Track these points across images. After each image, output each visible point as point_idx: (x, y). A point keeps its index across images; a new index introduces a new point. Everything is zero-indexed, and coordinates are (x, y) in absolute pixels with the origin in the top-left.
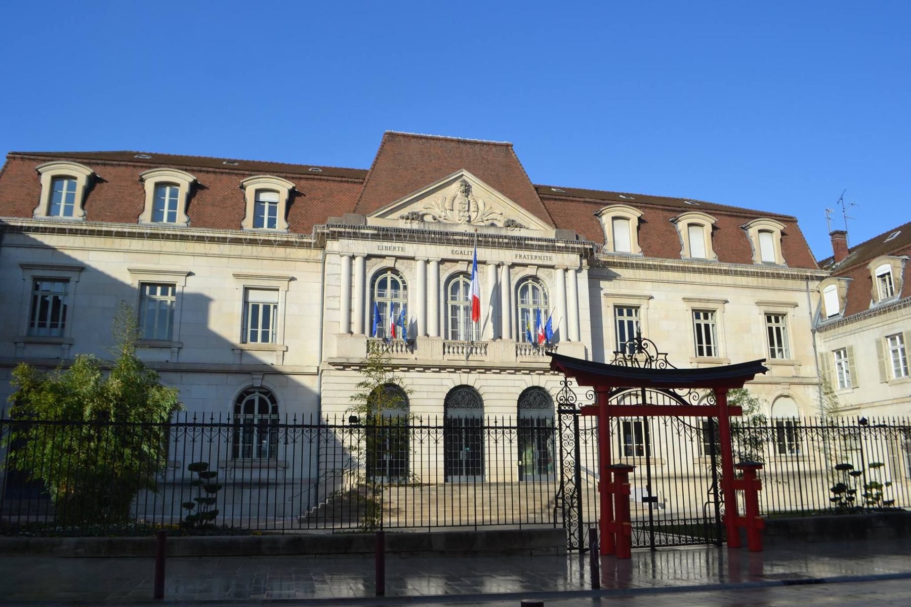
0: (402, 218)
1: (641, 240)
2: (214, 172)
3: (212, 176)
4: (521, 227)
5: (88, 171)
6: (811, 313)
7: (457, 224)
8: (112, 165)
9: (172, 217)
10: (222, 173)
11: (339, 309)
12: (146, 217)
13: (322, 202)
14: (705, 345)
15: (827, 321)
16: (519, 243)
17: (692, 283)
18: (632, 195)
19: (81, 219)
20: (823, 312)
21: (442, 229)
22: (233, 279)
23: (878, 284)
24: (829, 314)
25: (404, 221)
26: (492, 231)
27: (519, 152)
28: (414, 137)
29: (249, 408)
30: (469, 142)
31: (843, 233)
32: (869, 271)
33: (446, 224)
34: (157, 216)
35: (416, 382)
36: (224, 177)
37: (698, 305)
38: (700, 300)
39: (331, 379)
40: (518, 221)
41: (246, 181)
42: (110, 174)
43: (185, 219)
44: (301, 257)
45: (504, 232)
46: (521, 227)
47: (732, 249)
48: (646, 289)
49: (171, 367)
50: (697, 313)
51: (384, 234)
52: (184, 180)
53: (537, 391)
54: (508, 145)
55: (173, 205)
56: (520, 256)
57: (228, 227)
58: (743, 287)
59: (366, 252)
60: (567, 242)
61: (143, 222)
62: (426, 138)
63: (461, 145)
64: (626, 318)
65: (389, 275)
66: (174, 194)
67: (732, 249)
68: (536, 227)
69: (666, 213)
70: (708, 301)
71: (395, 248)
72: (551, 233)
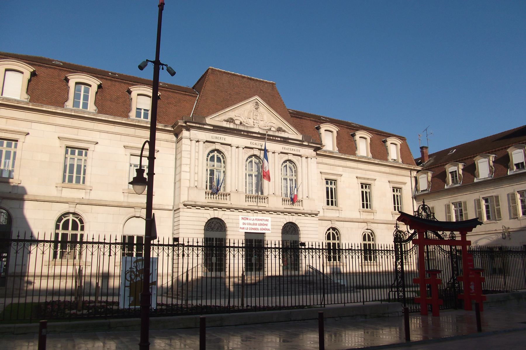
1: (339, 144)
2: (111, 80)
3: (109, 82)
4: (284, 131)
5: (31, 69)
7: (253, 127)
8: (46, 67)
9: (85, 106)
10: (116, 81)
11: (190, 172)
12: (69, 104)
13: (175, 106)
14: (365, 203)
15: (420, 193)
16: (285, 141)
18: (328, 118)
19: (94, 112)
21: (246, 129)
22: (124, 149)
23: (450, 176)
24: (421, 189)
25: (226, 122)
26: (270, 133)
27: (279, 88)
28: (224, 72)
29: (66, 226)
30: (253, 80)
31: (427, 148)
32: (445, 169)
33: (248, 127)
34: (76, 104)
35: (231, 217)
36: (117, 83)
38: (364, 179)
39: (185, 214)
40: (284, 128)
41: (132, 89)
42: (44, 73)
43: (95, 108)
44: (163, 138)
45: (277, 134)
46: (284, 131)
47: (379, 153)
48: (339, 171)
49: (86, 202)
50: (362, 185)
51: (217, 129)
52: (94, 83)
53: (216, 220)
54: (273, 84)
55: (86, 98)
57: (121, 116)
58: (384, 173)
59: (205, 139)
60: (309, 142)
61: (67, 107)
62: (231, 74)
63: (249, 81)
65: (216, 153)
66: (87, 91)
67: (379, 153)
68: (292, 133)
69: (348, 130)
71: (221, 138)
72: (300, 137)
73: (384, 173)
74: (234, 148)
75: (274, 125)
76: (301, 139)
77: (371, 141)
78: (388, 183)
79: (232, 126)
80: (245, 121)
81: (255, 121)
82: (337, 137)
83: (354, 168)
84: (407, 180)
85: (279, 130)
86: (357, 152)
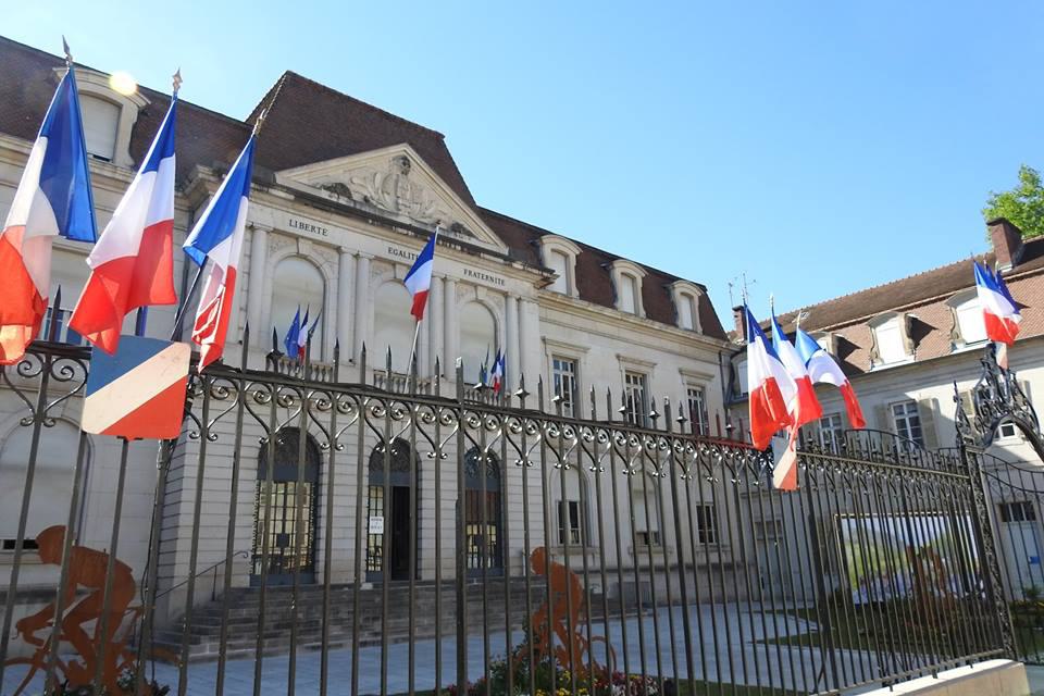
0: (327, 188)
4: (470, 234)
6: (723, 389)
17: (626, 341)
20: (736, 389)
37: (631, 367)
38: (633, 361)
46: (470, 234)
56: (470, 272)
58: (670, 352)
59: (272, 225)
64: (562, 373)
70: (640, 363)
71: (313, 228)
73: (670, 352)
74: (348, 260)
75: (443, 218)
76: (507, 253)
77: (643, 283)
78: (679, 376)
79: (343, 201)
80: (376, 197)
81: (400, 201)
82: (576, 267)
83: (612, 337)
84: (715, 370)
85: (457, 228)
86: (618, 305)
